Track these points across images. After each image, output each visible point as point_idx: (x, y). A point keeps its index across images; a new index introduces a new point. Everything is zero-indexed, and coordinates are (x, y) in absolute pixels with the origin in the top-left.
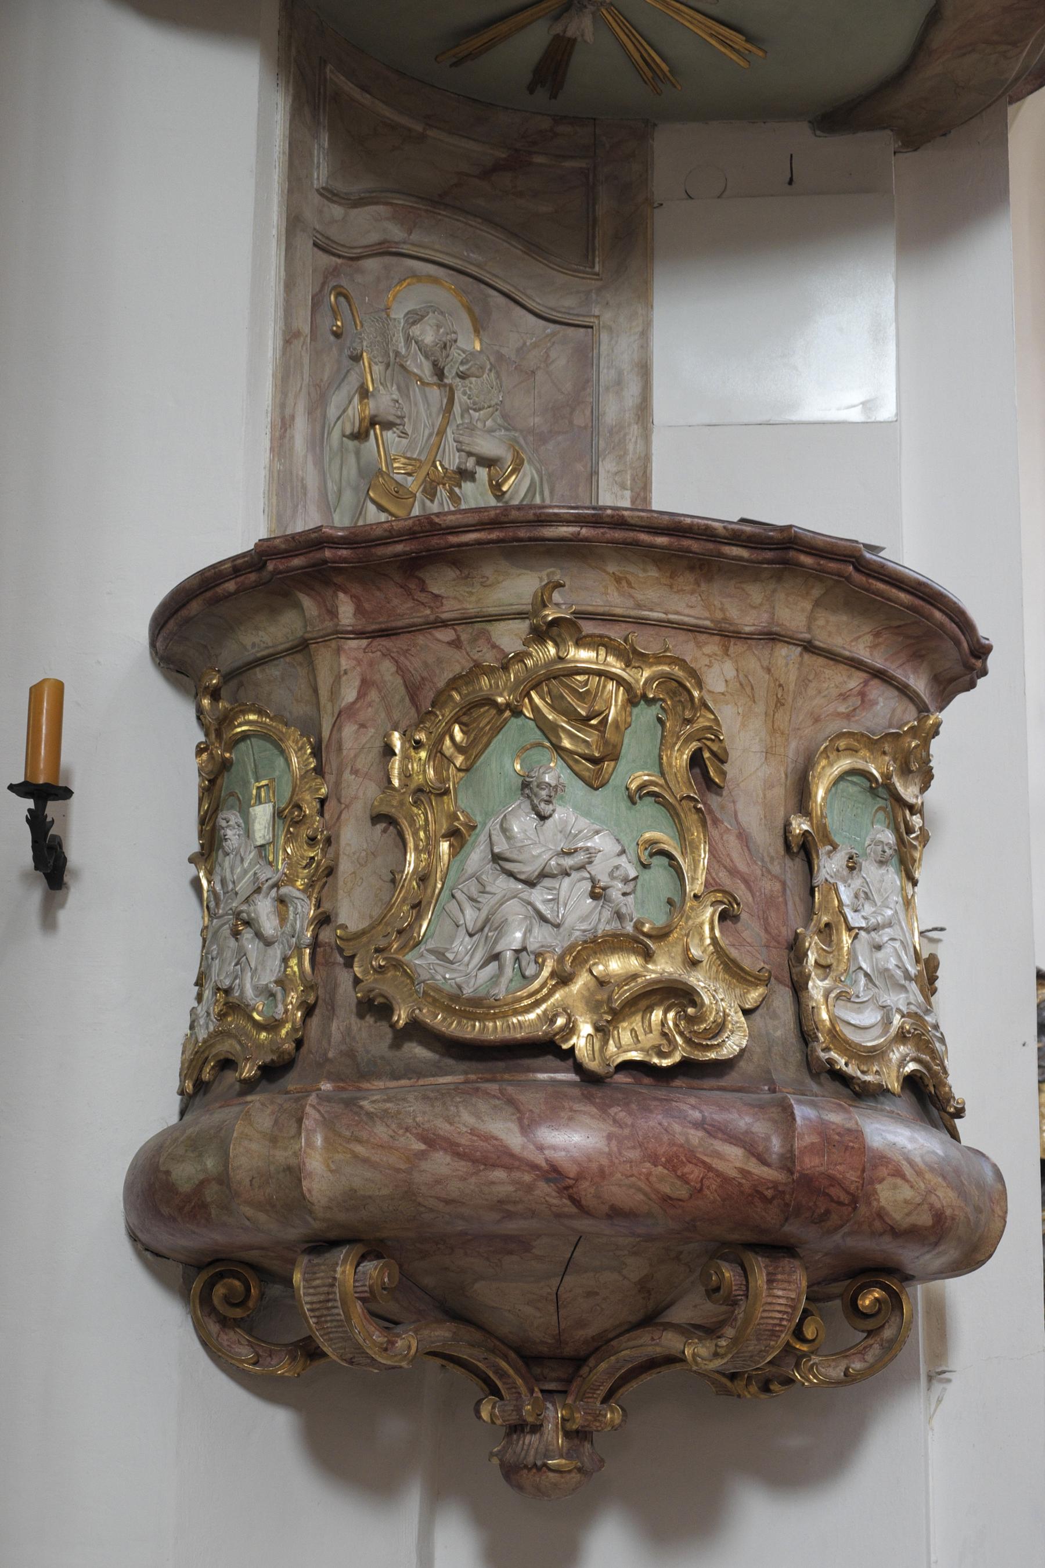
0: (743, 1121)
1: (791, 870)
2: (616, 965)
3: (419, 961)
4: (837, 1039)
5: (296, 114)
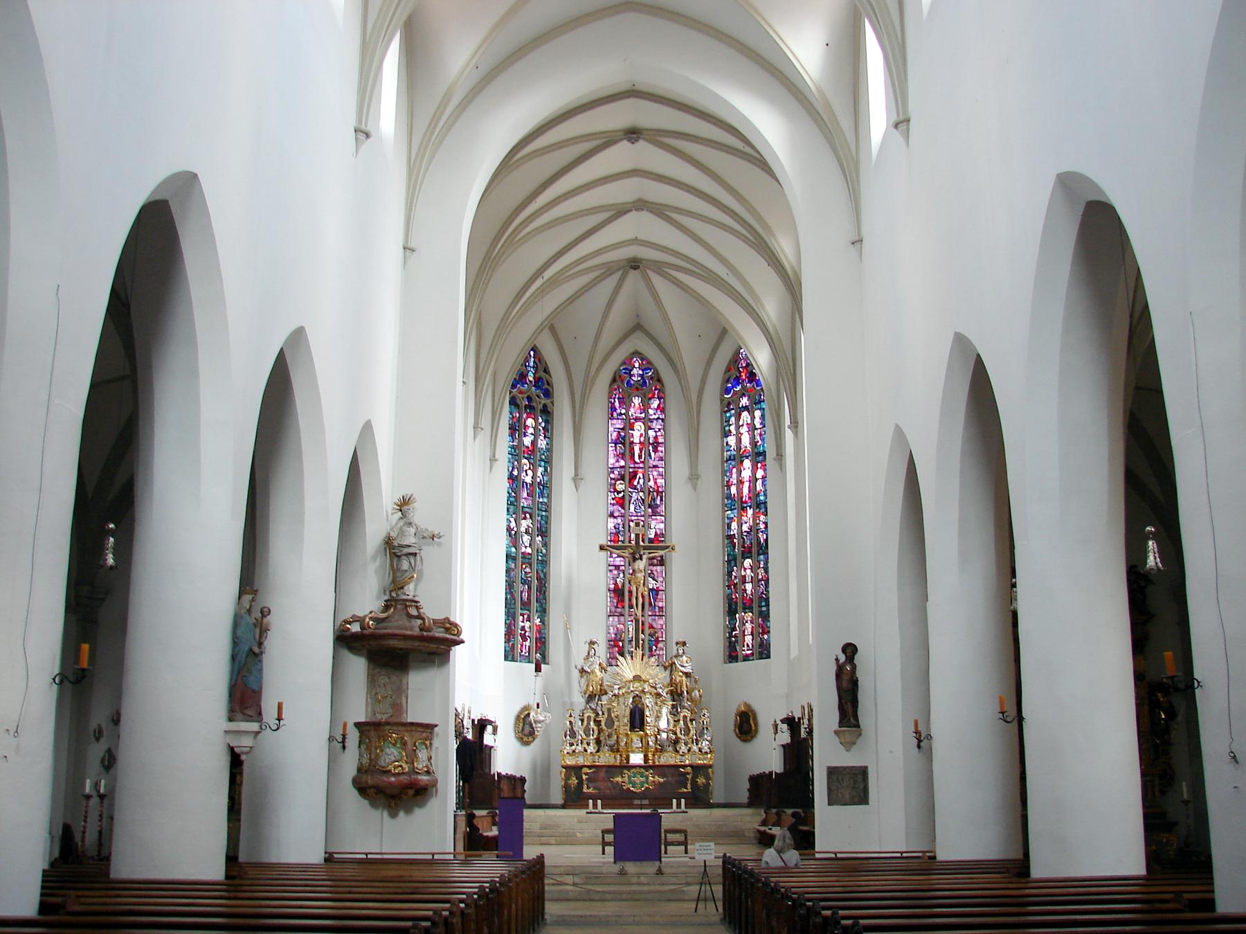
0: (406, 777)
1: (413, 753)
2: (397, 763)
3: (379, 762)
4: (417, 769)
5: (369, 663)
